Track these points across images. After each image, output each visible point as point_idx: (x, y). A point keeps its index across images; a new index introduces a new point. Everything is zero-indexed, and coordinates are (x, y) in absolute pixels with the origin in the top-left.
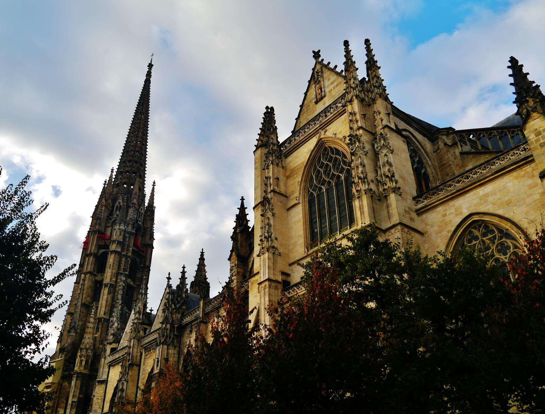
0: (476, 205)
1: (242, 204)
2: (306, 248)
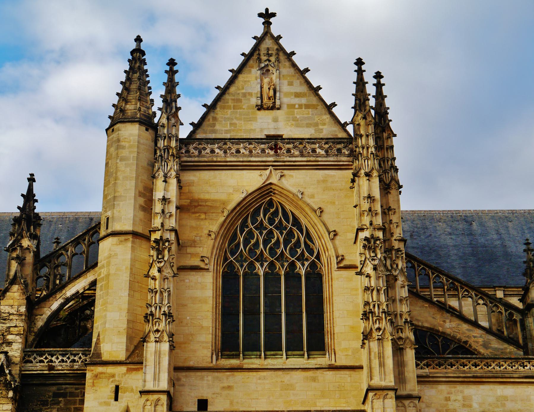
0: (490, 405)
1: (30, 189)
2: (214, 353)
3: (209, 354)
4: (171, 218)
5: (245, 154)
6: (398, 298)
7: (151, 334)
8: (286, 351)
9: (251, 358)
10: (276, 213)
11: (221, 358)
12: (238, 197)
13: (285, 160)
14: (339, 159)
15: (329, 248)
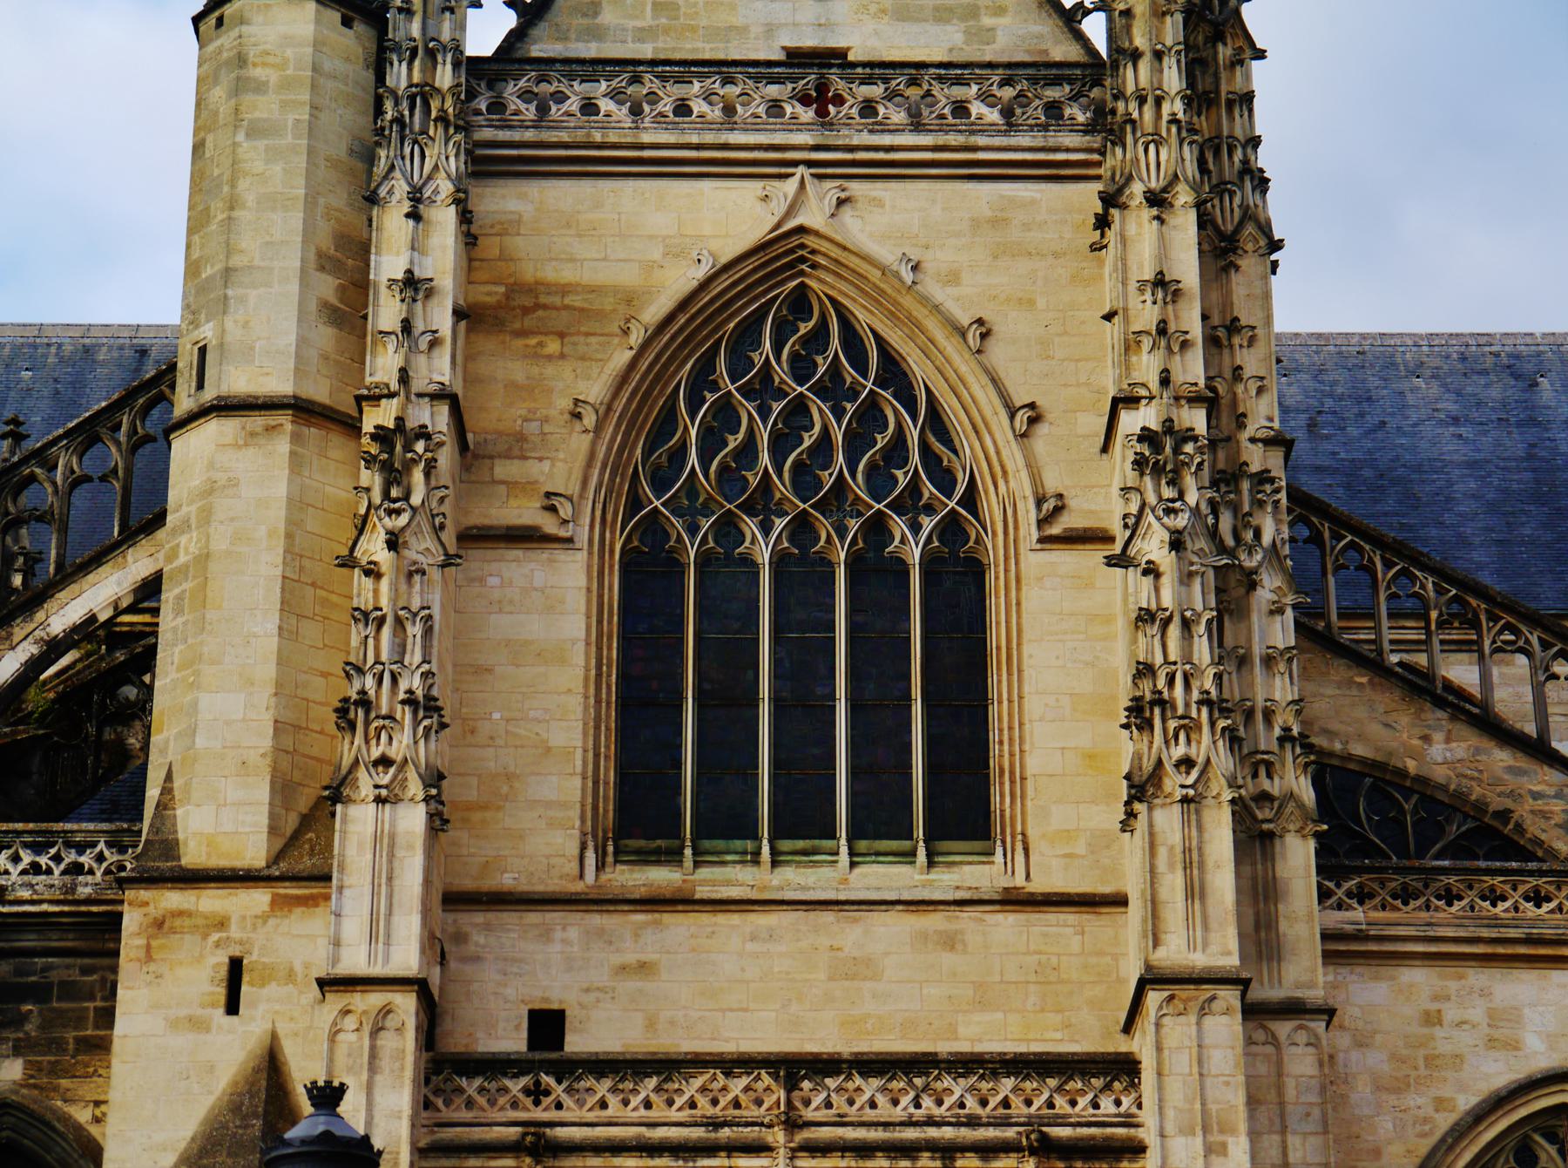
2: (591, 844)
3: (573, 849)
4: (436, 352)
5: (709, 118)
6: (1257, 651)
7: (362, 770)
8: (849, 840)
9: (723, 863)
10: (818, 338)
11: (616, 862)
12: (681, 279)
13: (855, 141)
14: (1051, 142)
15: (1010, 467)
